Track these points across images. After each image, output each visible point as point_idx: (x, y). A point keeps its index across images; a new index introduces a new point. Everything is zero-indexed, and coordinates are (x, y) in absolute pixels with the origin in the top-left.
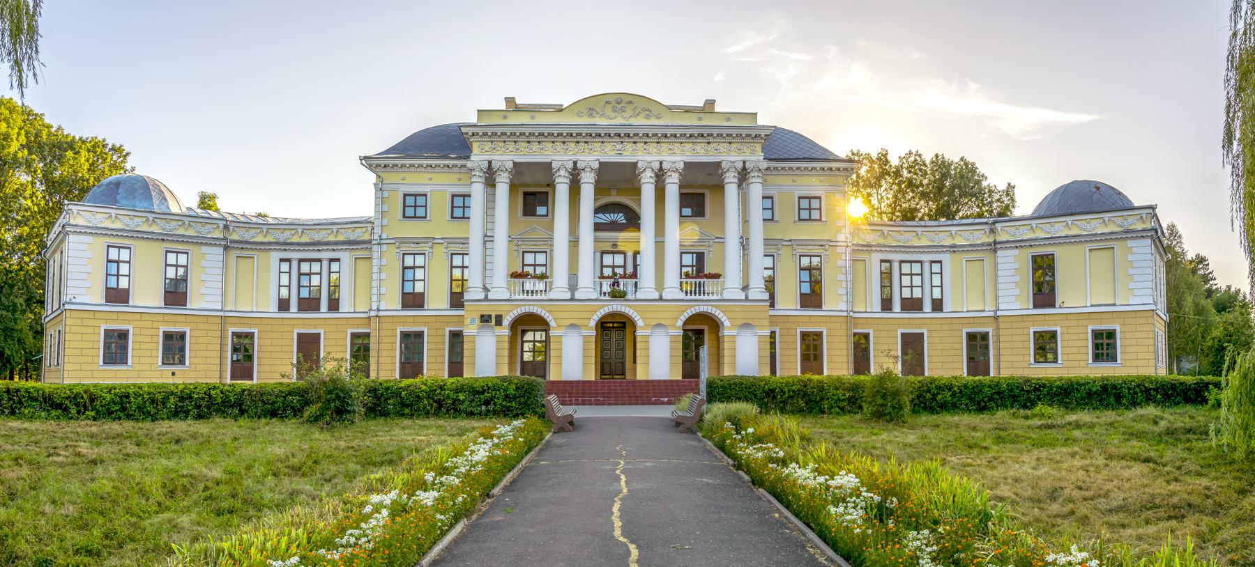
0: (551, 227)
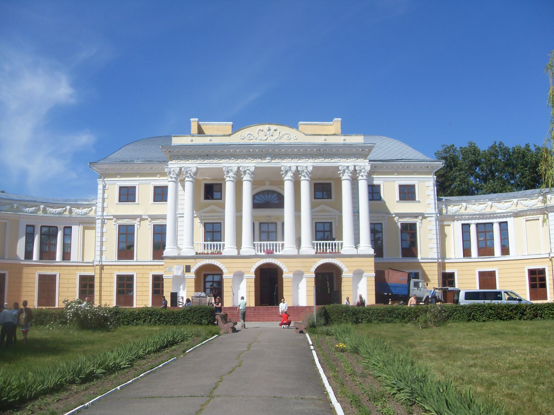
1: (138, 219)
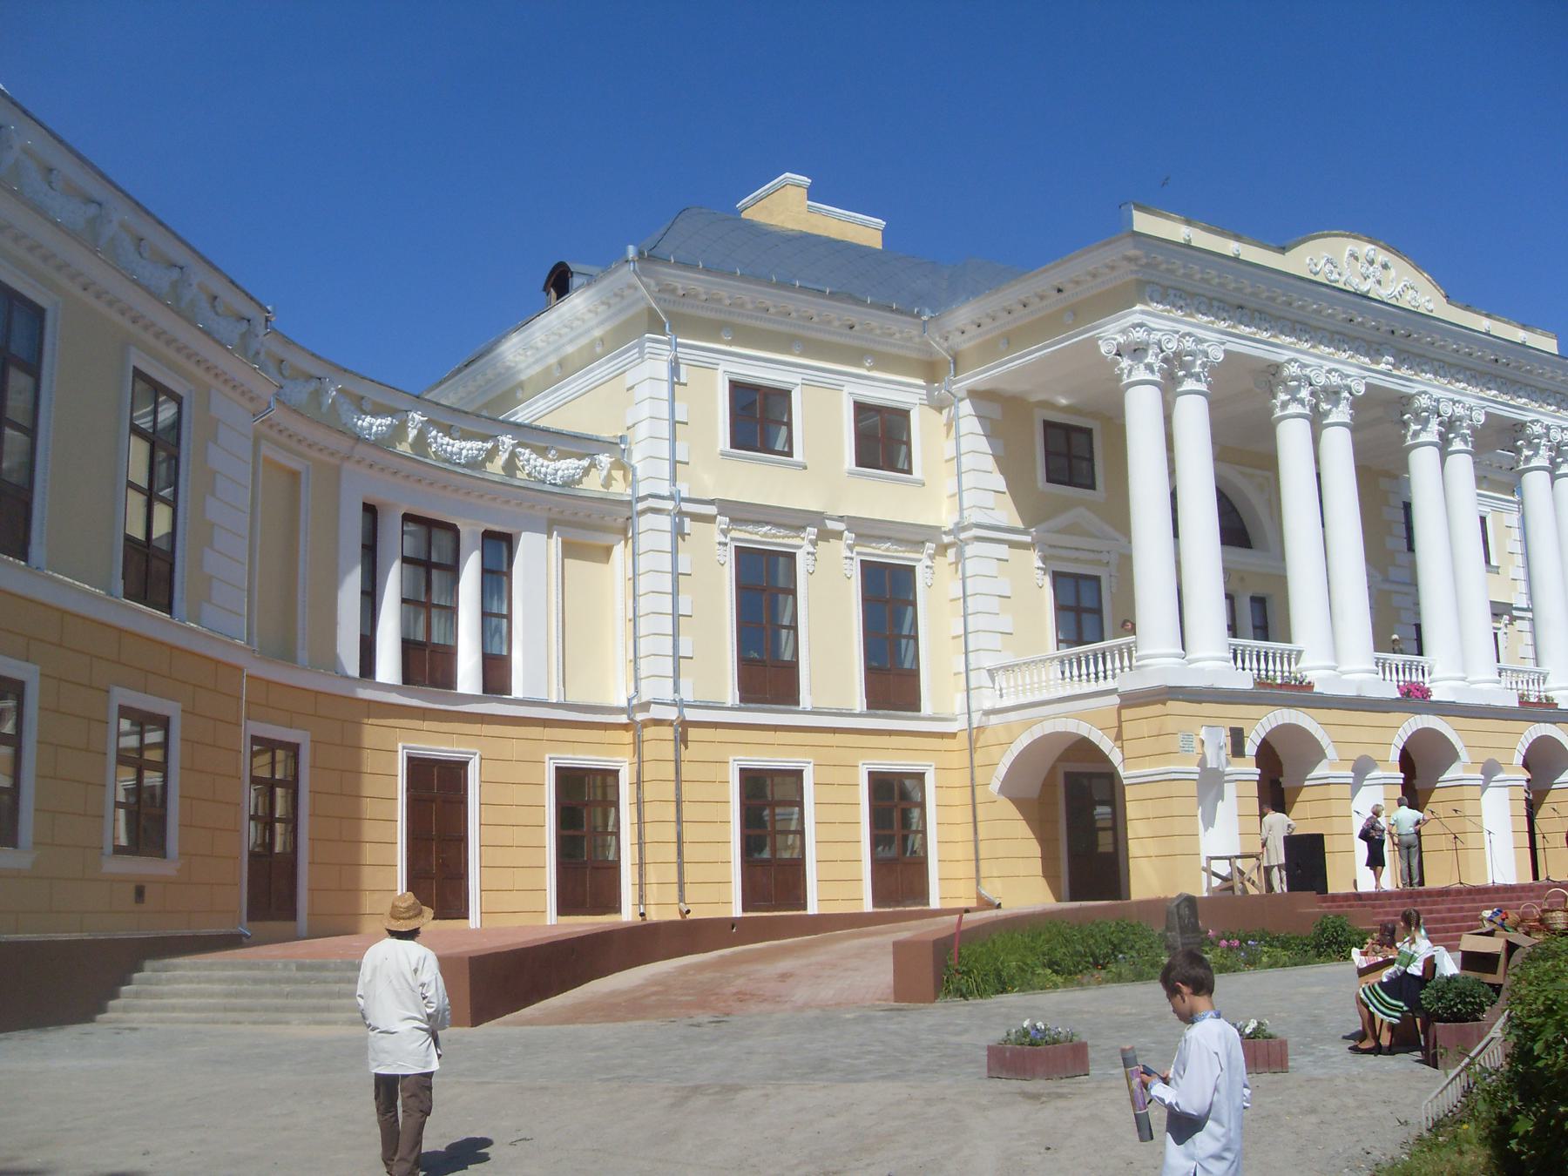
1: (812, 532)
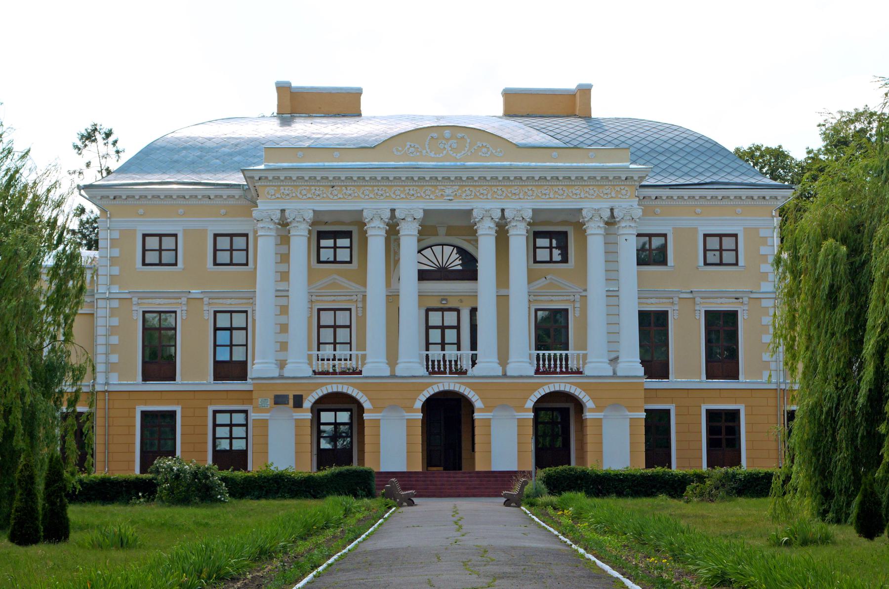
0: (361, 278)
1: (184, 300)
